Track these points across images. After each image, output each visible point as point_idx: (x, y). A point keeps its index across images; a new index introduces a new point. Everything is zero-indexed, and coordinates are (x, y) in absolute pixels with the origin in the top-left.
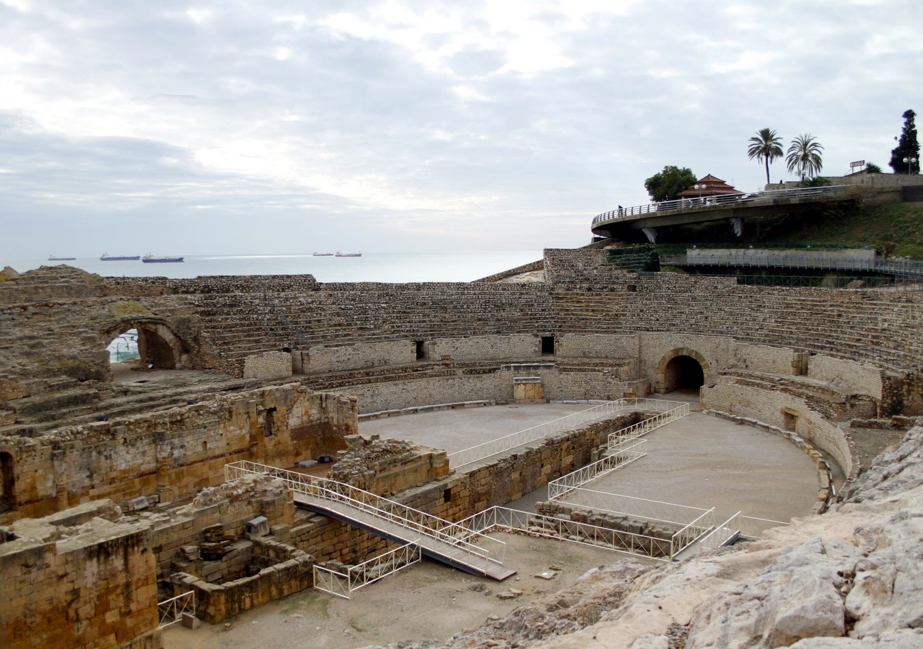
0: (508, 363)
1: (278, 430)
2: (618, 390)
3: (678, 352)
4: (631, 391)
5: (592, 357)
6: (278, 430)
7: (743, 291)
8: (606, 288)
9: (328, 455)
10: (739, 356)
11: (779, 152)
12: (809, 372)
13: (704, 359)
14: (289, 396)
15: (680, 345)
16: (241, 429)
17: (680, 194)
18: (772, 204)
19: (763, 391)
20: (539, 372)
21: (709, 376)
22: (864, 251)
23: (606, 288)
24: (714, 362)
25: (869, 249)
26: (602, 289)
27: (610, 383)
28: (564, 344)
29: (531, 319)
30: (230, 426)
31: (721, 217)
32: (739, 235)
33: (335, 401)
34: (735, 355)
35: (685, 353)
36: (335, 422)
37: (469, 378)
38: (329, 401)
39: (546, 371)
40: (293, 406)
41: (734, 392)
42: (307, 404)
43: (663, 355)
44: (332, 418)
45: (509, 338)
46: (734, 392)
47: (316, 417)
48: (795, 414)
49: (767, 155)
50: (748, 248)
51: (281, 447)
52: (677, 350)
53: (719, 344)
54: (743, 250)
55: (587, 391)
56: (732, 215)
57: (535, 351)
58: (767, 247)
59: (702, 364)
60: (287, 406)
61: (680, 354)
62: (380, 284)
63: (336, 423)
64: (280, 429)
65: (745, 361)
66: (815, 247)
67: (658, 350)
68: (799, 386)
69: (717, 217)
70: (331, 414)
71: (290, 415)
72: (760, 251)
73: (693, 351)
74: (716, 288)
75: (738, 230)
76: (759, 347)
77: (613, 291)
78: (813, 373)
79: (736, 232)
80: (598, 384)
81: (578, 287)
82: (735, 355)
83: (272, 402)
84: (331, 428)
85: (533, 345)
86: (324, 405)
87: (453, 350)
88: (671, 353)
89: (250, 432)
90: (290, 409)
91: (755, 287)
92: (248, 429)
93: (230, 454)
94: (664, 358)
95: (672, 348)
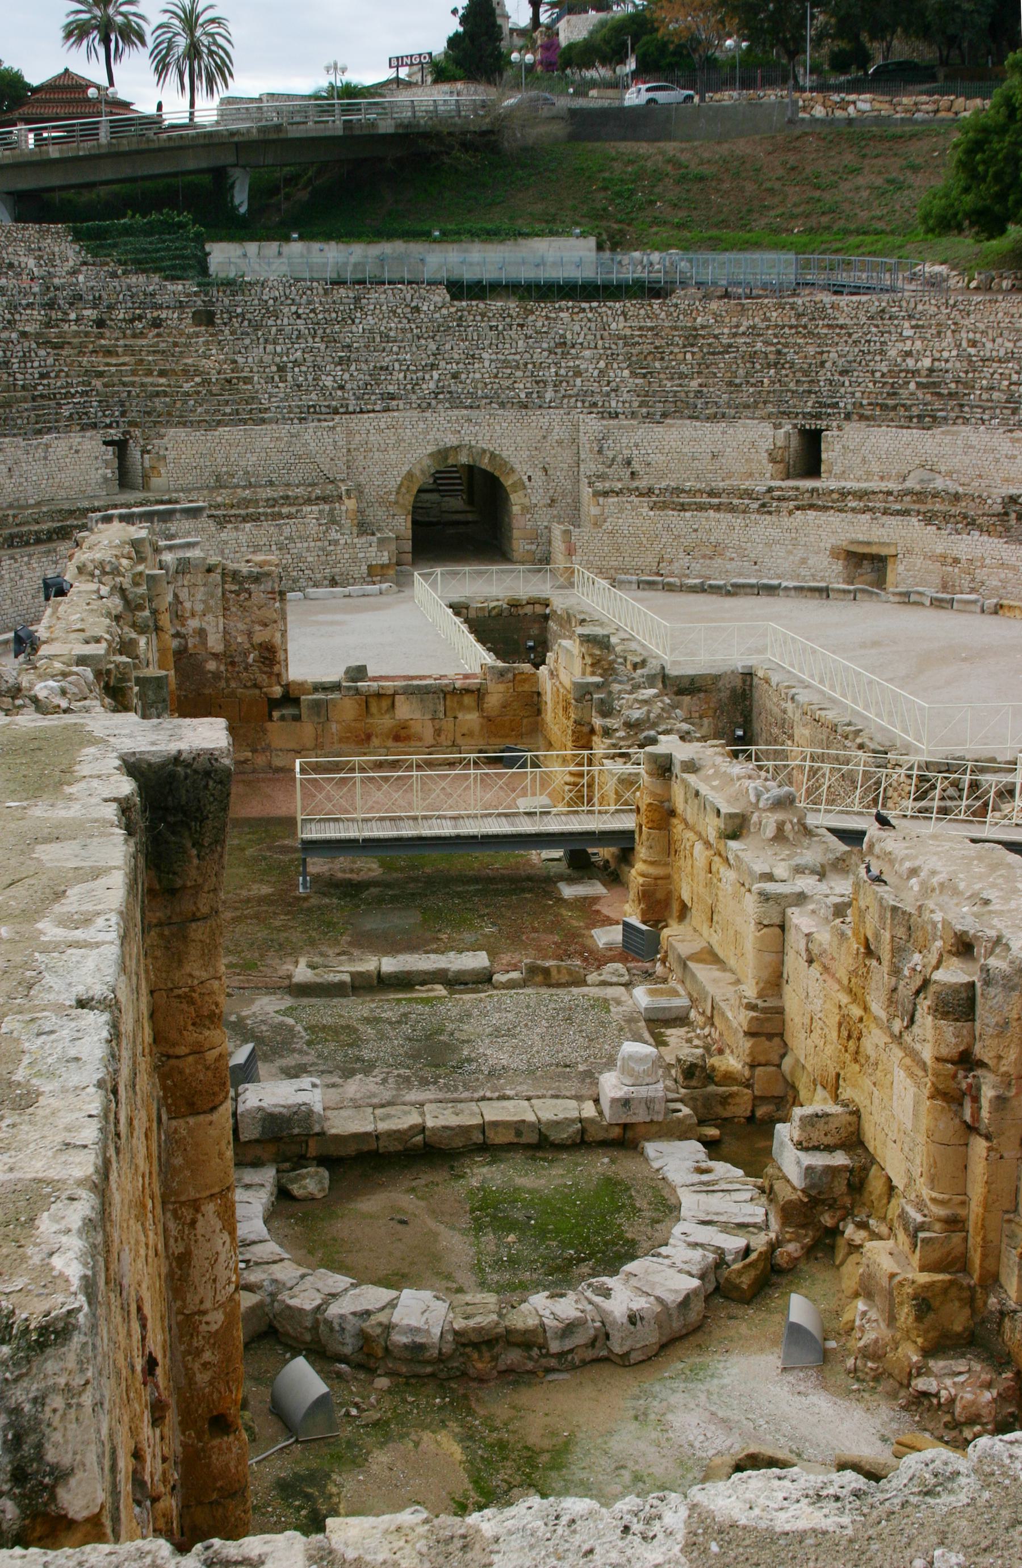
0: (107, 508)
2: (355, 560)
3: (446, 458)
4: (385, 560)
5: (237, 486)
7: (483, 315)
8: (140, 318)
10: (610, 454)
11: (131, 34)
12: (823, 468)
13: (512, 470)
15: (451, 440)
17: (16, 115)
18: (340, 133)
19: (738, 521)
20: (173, 527)
21: (526, 510)
22: (572, 241)
23: (140, 318)
24: (538, 475)
25: (583, 235)
26: (132, 321)
27: (336, 542)
28: (171, 455)
29: (34, 399)
31: (204, 165)
32: (243, 210)
33: (216, 577)
34: (600, 452)
35: (464, 459)
36: (215, 642)
37: (30, 556)
39: (187, 524)
41: (668, 529)
43: (406, 469)
44: (202, 633)
45: (47, 446)
46: (668, 529)
48: (884, 551)
49: (106, 41)
50: (287, 239)
52: (443, 454)
53: (549, 431)
54: (275, 245)
55: (285, 568)
56: (231, 160)
57: (106, 479)
58: (328, 236)
59: (508, 482)
61: (451, 461)
63: (219, 648)
65: (629, 463)
66: (448, 237)
67: (393, 456)
68: (835, 496)
69: (192, 165)
70: (193, 624)
72: (316, 246)
73: (484, 451)
74: (417, 309)
75: (241, 199)
76: (671, 426)
77: (159, 326)
78: (837, 469)
79: (237, 202)
80: (308, 549)
81: (73, 316)
82: (600, 452)
84: (198, 667)
85: (99, 463)
88: (427, 462)
91: (512, 305)
94: (410, 475)
95: (431, 449)
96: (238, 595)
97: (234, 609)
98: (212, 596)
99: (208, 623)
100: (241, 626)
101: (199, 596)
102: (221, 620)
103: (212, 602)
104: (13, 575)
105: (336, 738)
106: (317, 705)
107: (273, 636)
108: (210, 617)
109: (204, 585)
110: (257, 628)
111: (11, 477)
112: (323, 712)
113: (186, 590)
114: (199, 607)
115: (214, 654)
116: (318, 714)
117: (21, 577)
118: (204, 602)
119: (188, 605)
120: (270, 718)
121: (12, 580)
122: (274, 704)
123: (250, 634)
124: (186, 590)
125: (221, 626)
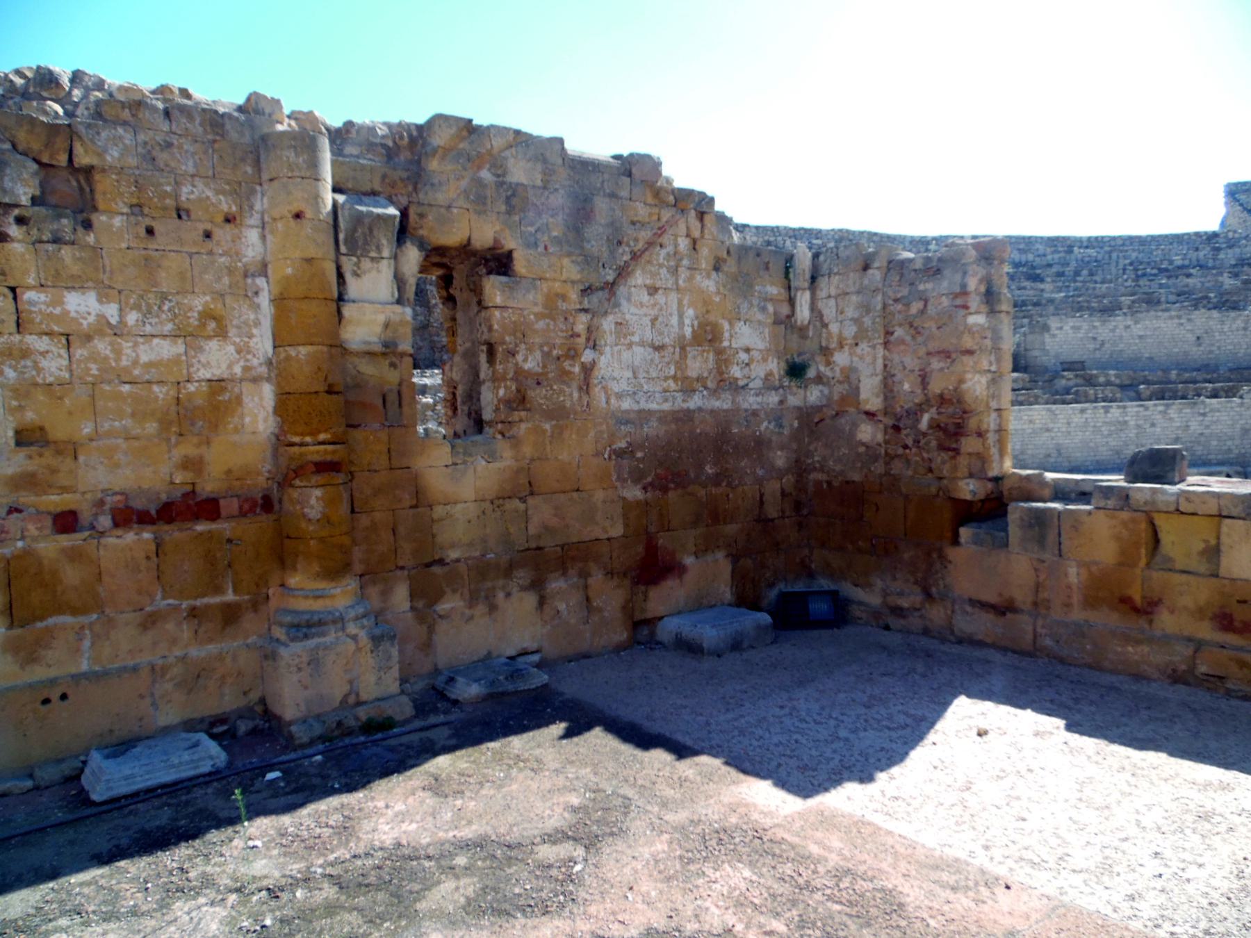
1: (520, 401)
6: (520, 401)
9: (825, 584)
14: (601, 205)
16: (189, 334)
30: (58, 281)
37: (1167, 406)
38: (827, 287)
40: (623, 273)
42: (709, 284)
47: (759, 371)
51: (541, 512)
60: (588, 260)
62: (876, 234)
64: (538, 395)
71: (608, 324)
83: (479, 200)
86: (803, 313)
87: (1091, 346)
89: (278, 370)
90: (611, 287)
92: (263, 343)
93: (66, 522)
96: (907, 305)
97: (899, 332)
98: (867, 309)
99: (861, 358)
100: (911, 362)
101: (850, 312)
102: (881, 351)
103: (867, 321)
104: (1141, 422)
105: (1076, 599)
106: (1040, 521)
107: (961, 381)
108: (864, 347)
109: (858, 292)
110: (936, 364)
111: (1200, 345)
112: (1051, 537)
113: (832, 302)
114: (850, 331)
115: (868, 413)
116: (1041, 542)
117: (1153, 425)
118: (856, 321)
119: (834, 328)
120: (955, 541)
121: (1138, 426)
122: (968, 513)
123: (924, 380)
124: (832, 302)
125: (880, 362)
